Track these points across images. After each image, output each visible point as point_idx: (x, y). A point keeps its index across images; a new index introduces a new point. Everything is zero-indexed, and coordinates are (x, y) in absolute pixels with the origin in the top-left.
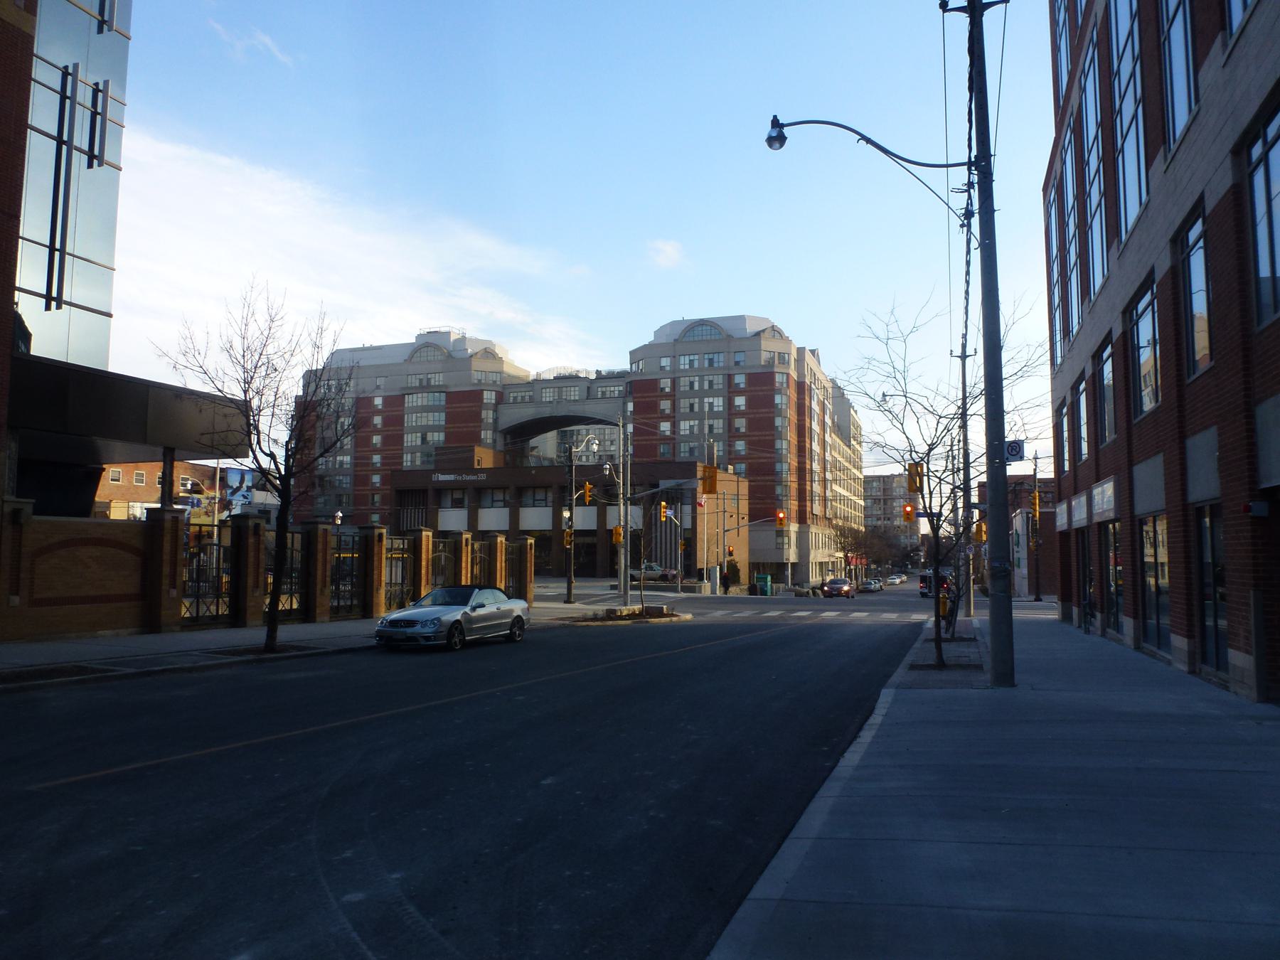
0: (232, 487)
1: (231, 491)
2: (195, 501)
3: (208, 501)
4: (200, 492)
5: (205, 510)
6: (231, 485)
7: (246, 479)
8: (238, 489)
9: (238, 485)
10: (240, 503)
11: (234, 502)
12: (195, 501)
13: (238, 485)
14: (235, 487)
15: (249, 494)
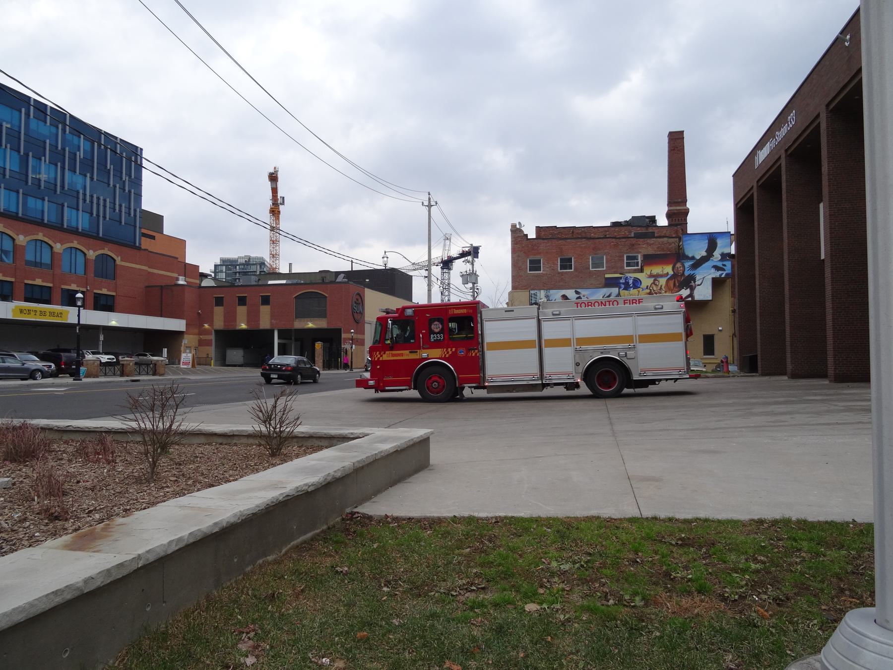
0: (693, 258)
1: (691, 263)
2: (631, 282)
3: (652, 280)
4: (641, 271)
5: (648, 291)
6: (690, 255)
7: (719, 245)
8: (704, 260)
9: (704, 254)
10: (710, 277)
11: (698, 278)
12: (631, 282)
13: (704, 254)
14: (698, 257)
15: (724, 263)
